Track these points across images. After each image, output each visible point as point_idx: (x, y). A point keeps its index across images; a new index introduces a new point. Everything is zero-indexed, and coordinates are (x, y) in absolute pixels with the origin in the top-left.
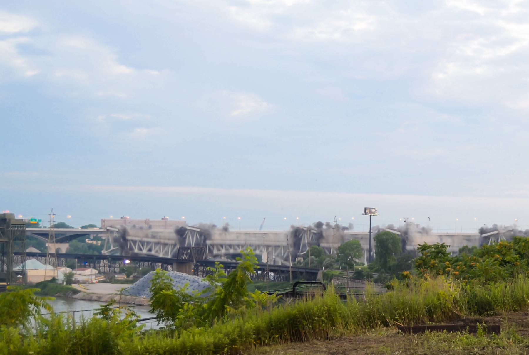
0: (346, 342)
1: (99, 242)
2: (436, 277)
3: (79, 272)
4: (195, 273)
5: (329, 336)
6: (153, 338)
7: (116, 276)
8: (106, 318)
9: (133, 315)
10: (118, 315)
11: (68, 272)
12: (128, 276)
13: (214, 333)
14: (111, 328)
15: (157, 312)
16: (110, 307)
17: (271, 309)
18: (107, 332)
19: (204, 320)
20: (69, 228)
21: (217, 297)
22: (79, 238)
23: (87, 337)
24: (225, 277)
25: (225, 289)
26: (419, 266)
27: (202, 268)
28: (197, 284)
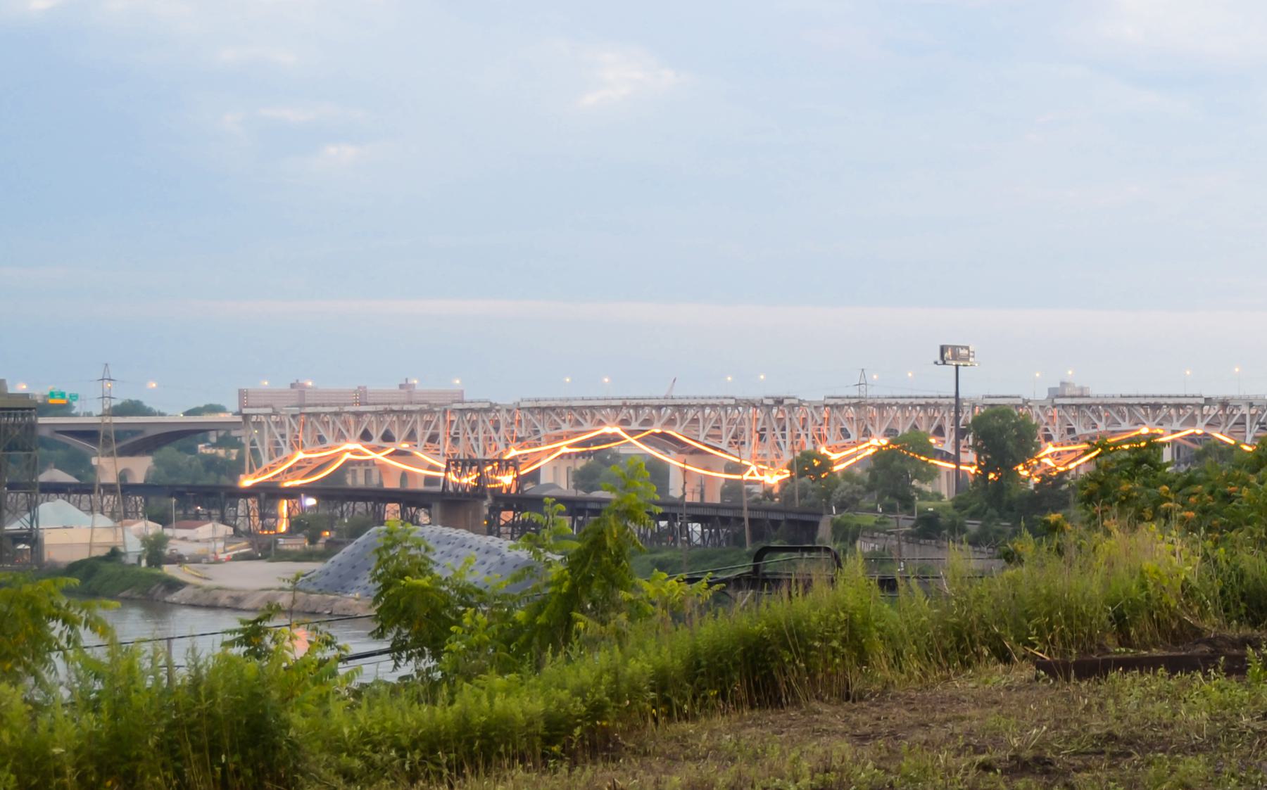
0: (899, 705)
1: (234, 451)
2: (1134, 529)
3: (181, 533)
4: (492, 529)
5: (852, 691)
6: (382, 705)
7: (281, 541)
8: (257, 652)
9: (328, 643)
10: (287, 644)
11: (151, 532)
12: (313, 540)
13: (545, 690)
14: (270, 681)
15: (391, 636)
16: (267, 624)
17: (696, 623)
18: (259, 690)
19: (518, 655)
20: (154, 414)
21: (550, 590)
22: (179, 442)
23: (206, 705)
24: (571, 538)
25: (572, 569)
26: (1089, 499)
27: (511, 514)
28: (497, 558)
